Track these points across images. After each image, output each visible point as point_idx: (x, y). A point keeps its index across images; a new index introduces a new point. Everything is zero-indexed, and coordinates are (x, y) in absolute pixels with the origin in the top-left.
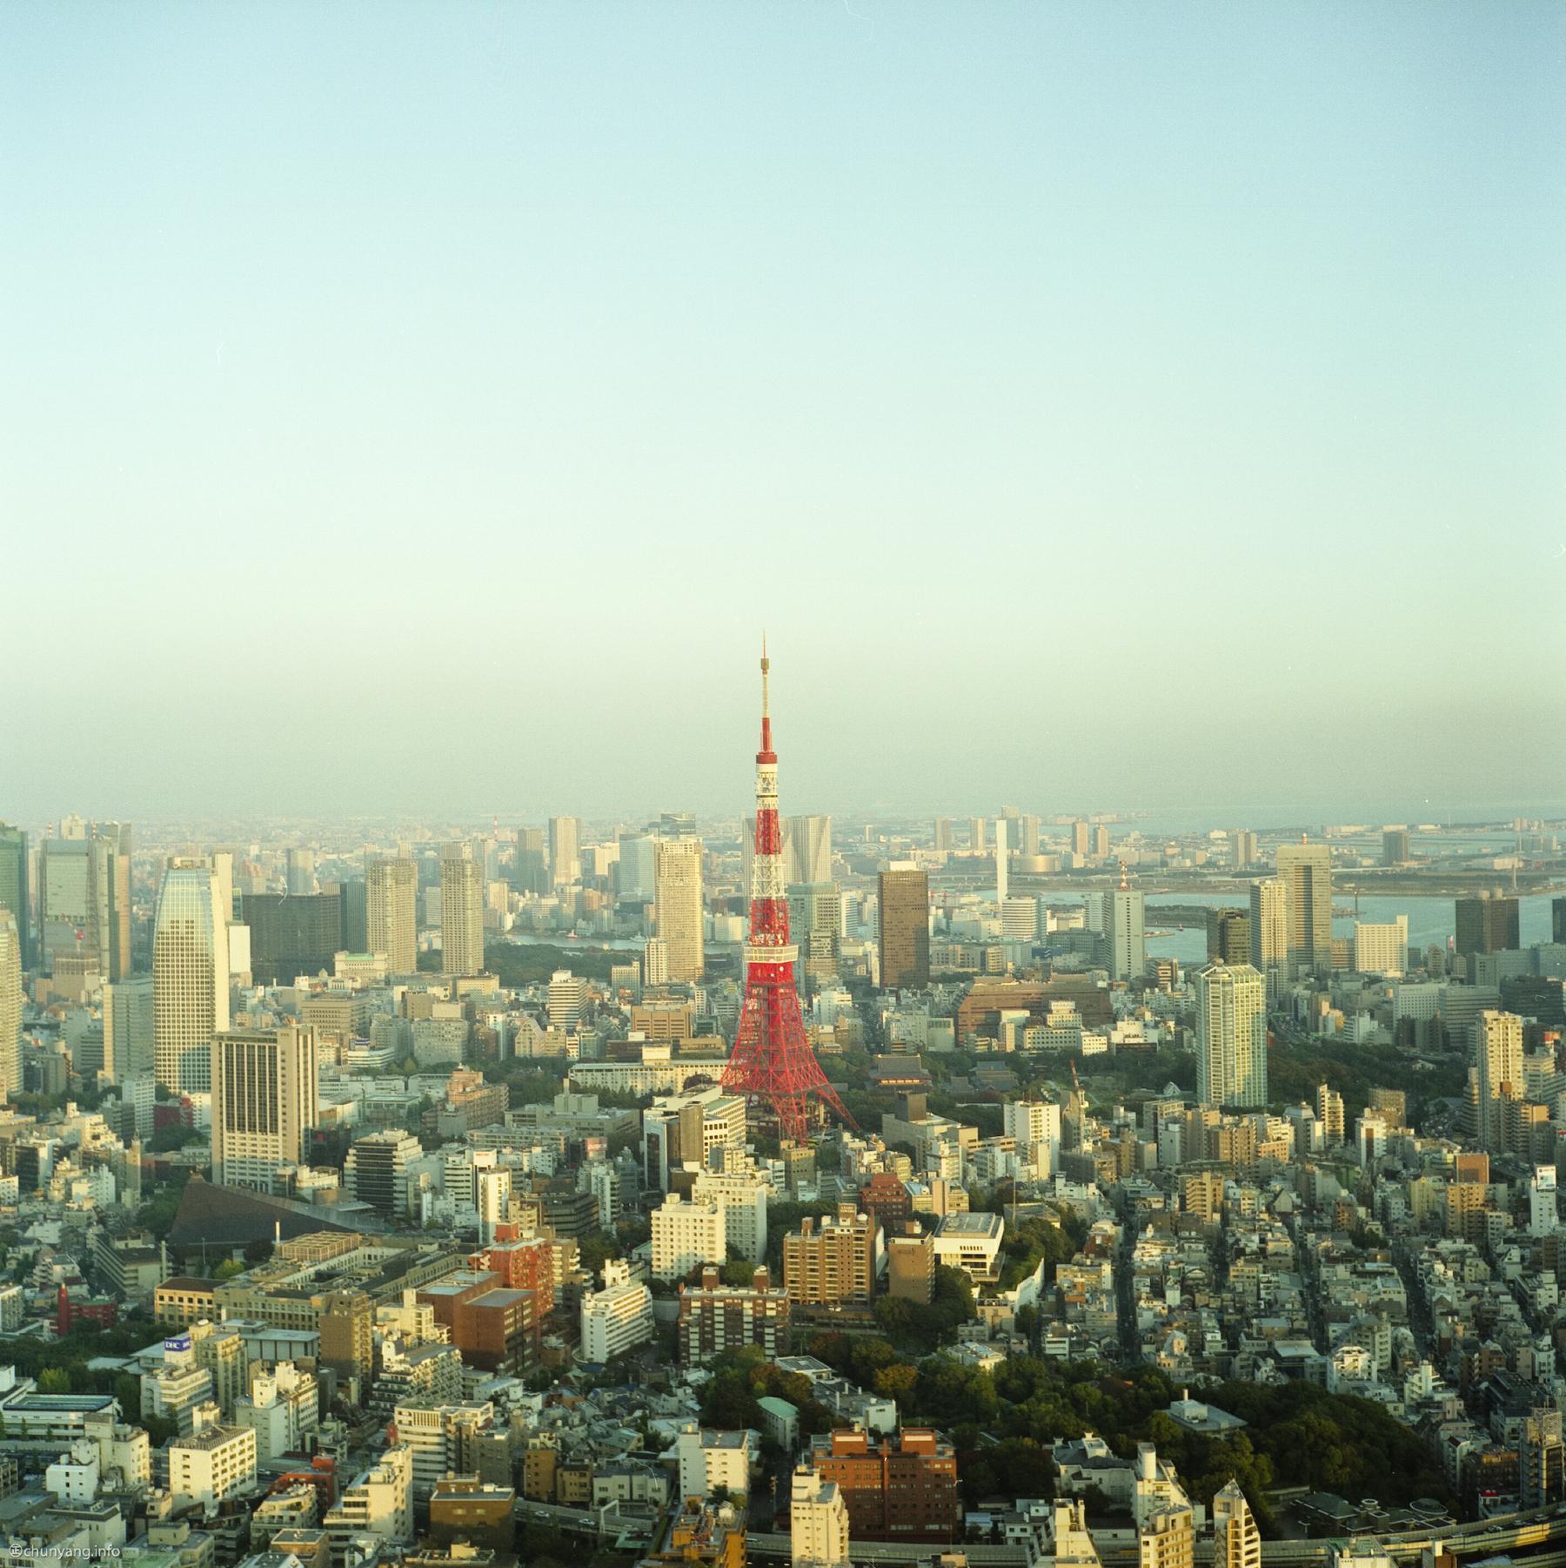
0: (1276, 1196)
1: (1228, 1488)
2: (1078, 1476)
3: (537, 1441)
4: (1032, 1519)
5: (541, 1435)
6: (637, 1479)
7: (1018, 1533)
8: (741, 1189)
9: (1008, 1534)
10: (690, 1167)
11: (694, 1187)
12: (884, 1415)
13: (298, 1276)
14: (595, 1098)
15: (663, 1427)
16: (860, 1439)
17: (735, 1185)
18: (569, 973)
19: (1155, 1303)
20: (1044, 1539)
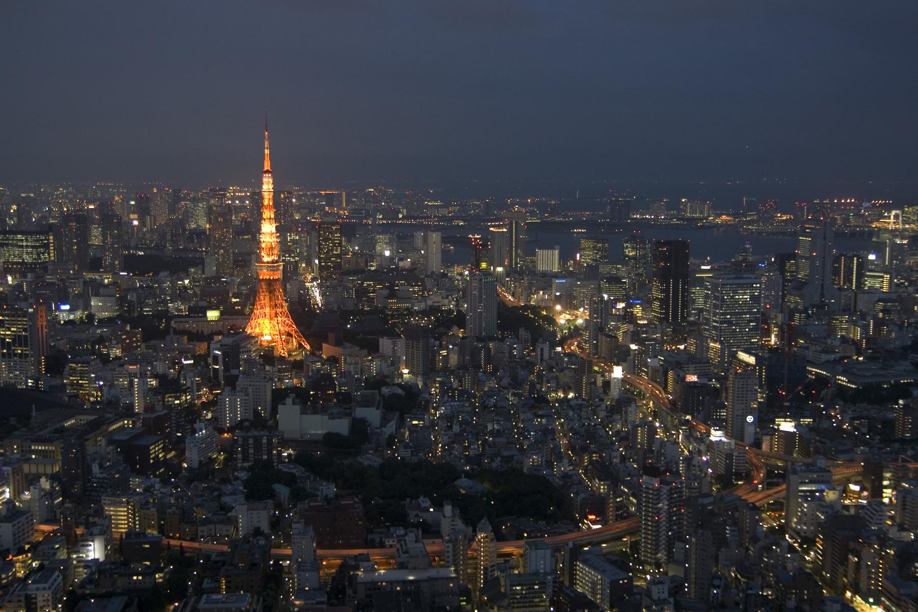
0: (501, 380)
1: (483, 521)
2: (417, 516)
3: (171, 511)
4: (397, 536)
5: (173, 508)
6: (218, 526)
7: (391, 543)
8: (259, 384)
9: (387, 543)
10: (234, 372)
11: (237, 383)
12: (330, 489)
13: (46, 431)
14: (186, 337)
15: (227, 499)
16: (321, 504)
17: (257, 381)
18: (168, 272)
19: (449, 432)
20: (404, 546)
